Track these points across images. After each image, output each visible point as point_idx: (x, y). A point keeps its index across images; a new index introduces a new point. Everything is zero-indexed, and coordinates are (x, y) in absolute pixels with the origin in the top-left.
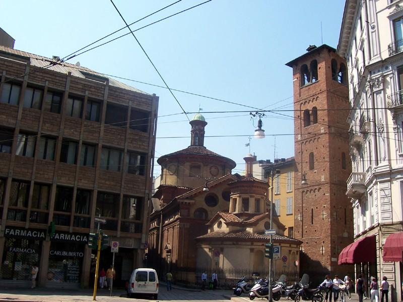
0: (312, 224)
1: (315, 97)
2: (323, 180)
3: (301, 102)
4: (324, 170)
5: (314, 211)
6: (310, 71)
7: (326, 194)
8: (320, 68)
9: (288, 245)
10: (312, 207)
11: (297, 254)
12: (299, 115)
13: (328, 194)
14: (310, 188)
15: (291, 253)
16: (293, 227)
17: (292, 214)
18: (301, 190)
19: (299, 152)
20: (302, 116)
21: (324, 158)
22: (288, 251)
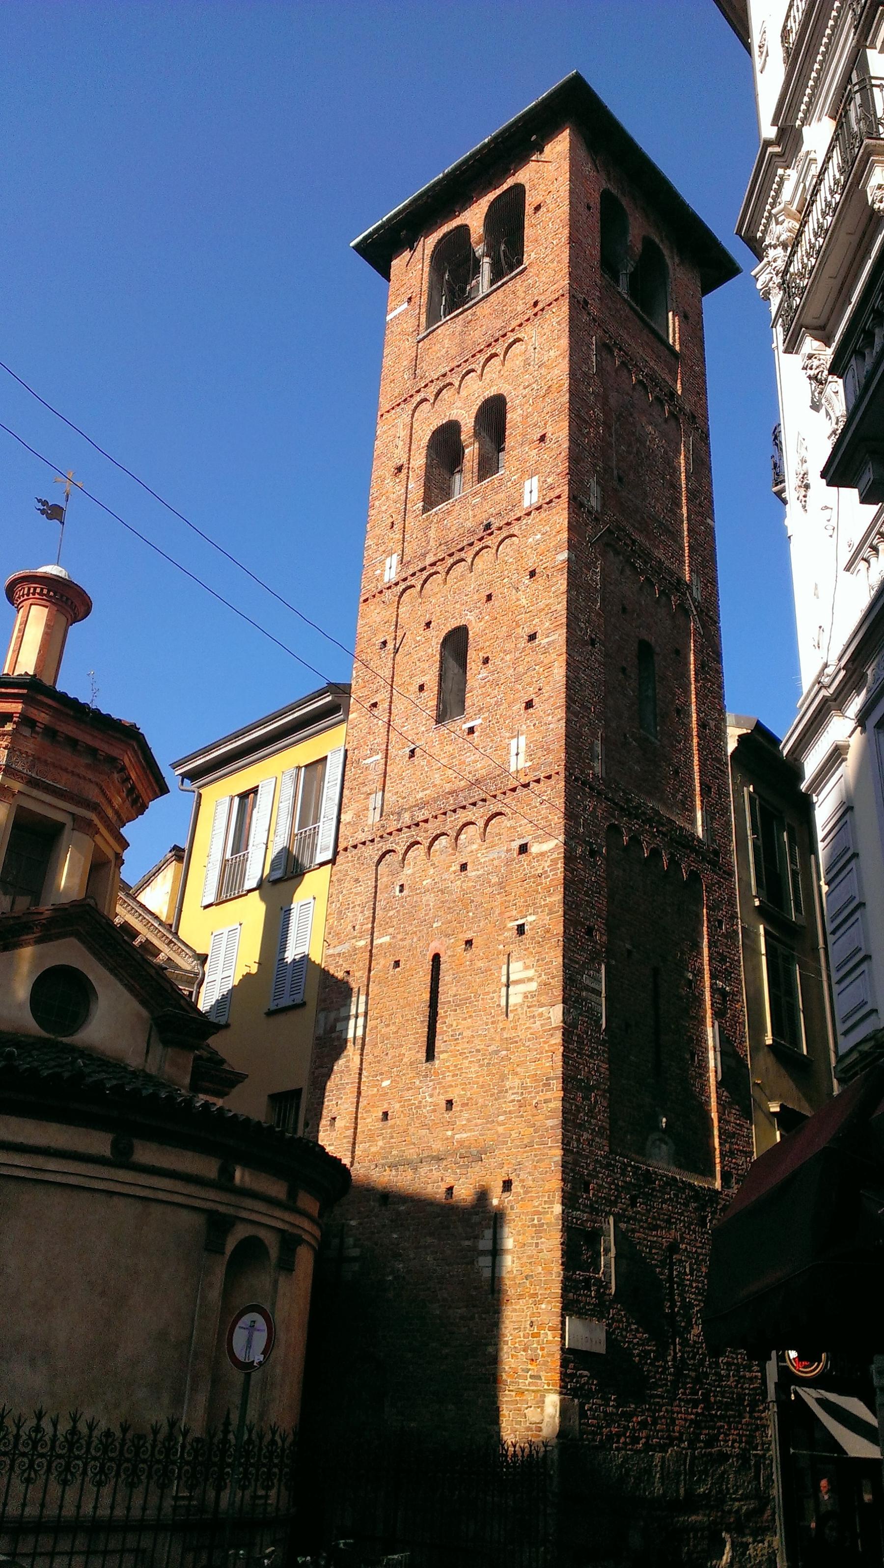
0: (430, 1055)
1: (499, 349)
2: (518, 762)
3: (418, 398)
4: (529, 705)
5: (446, 977)
6: (479, 250)
7: (535, 849)
8: (538, 208)
9: (208, 1167)
10: (435, 946)
11: (287, 1265)
12: (404, 460)
13: (551, 844)
14: (433, 828)
15: (230, 1245)
16: (297, 1093)
17: (303, 1005)
18: (372, 852)
19: (384, 643)
20: (419, 460)
21: (532, 637)
22: (198, 1220)
